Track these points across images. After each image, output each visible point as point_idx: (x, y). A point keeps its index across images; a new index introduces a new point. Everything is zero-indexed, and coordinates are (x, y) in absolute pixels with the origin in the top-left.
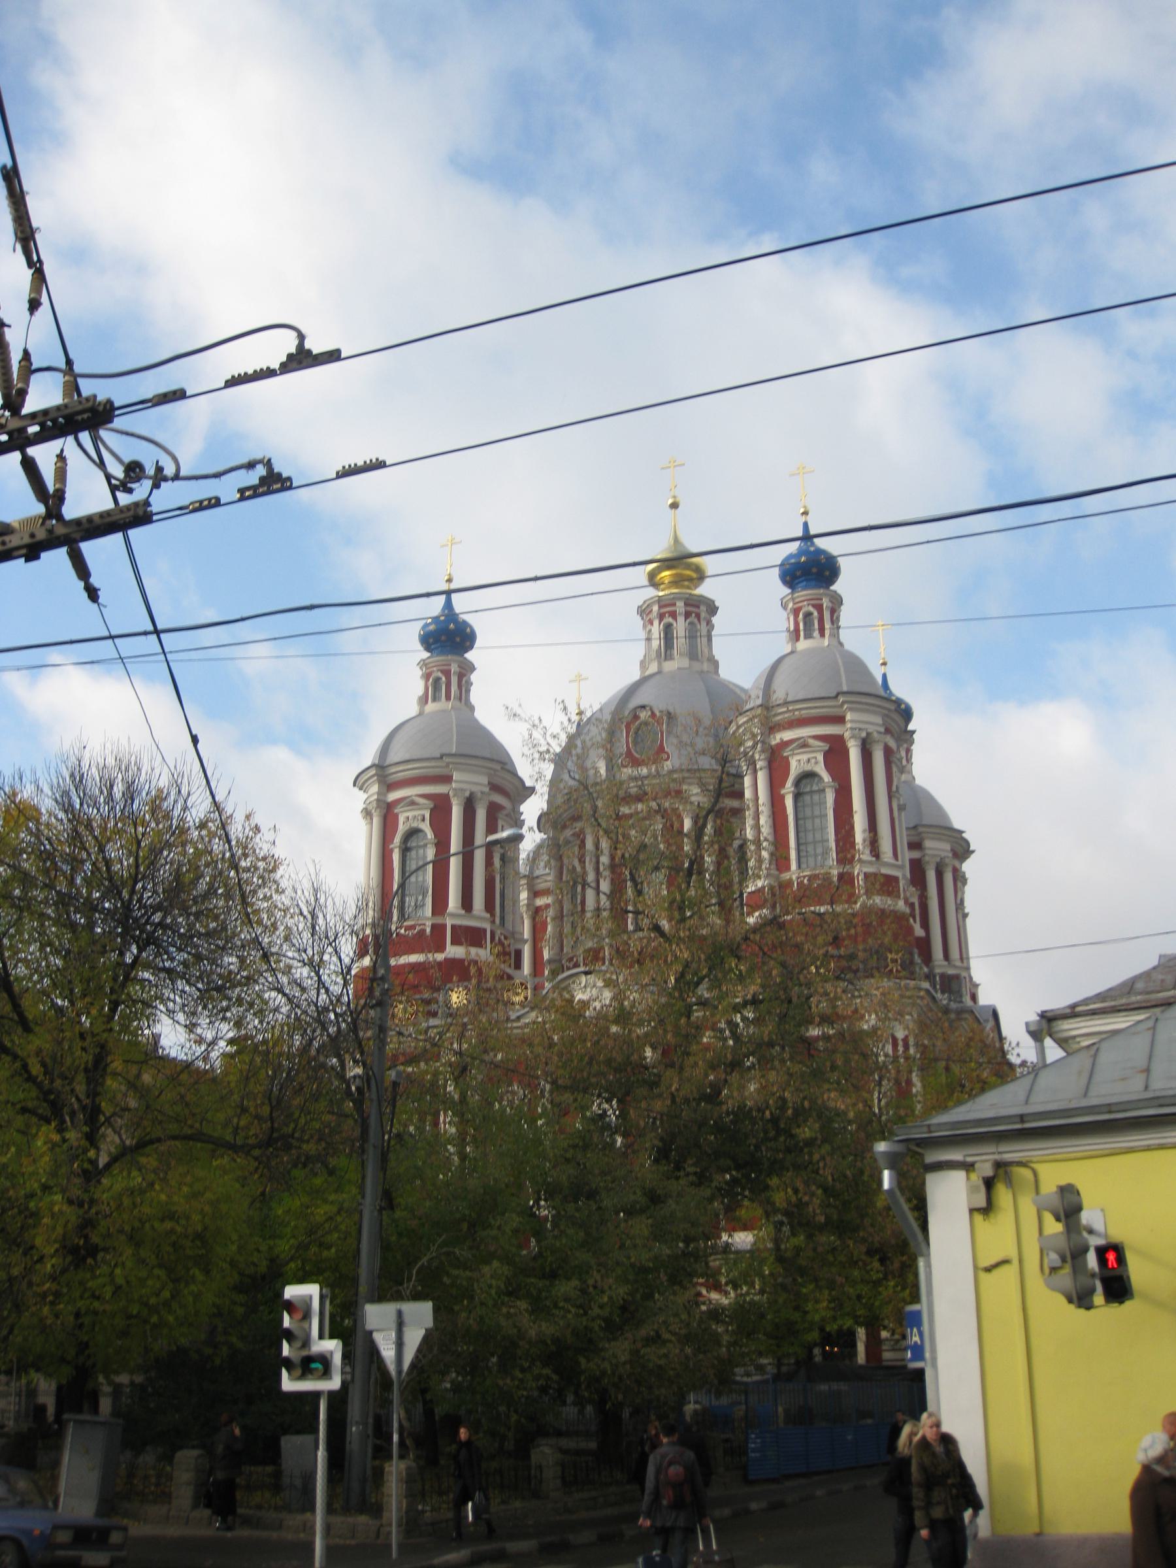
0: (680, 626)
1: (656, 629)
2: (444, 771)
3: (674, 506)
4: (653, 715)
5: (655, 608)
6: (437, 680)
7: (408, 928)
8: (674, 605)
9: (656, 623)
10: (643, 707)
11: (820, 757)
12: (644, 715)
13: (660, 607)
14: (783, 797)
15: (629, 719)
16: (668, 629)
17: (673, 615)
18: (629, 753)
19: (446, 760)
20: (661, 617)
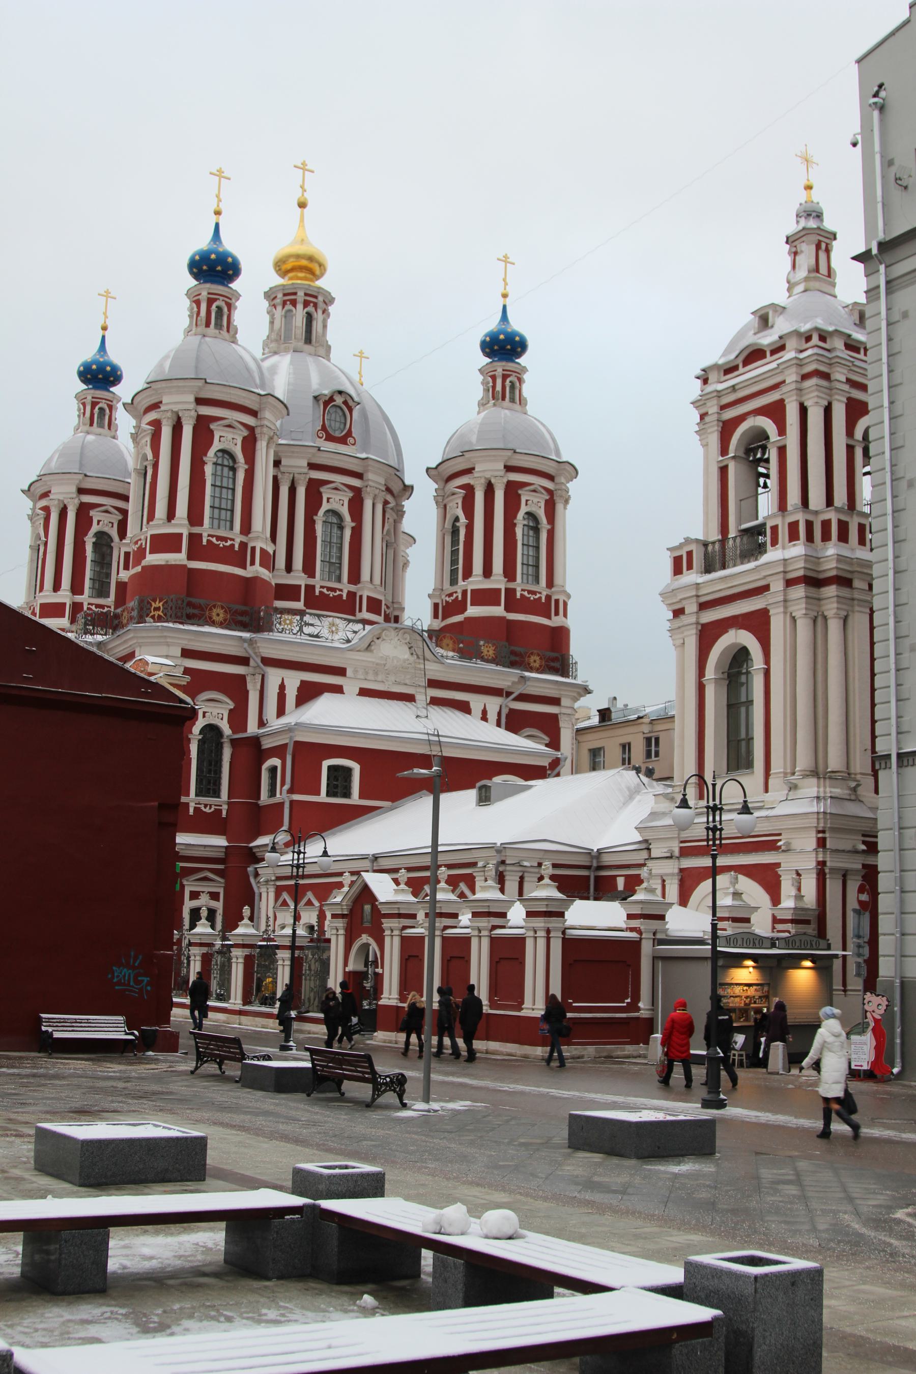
0: (319, 316)
1: (300, 313)
2: (255, 407)
3: (302, 205)
4: (345, 403)
5: (301, 294)
6: (219, 309)
7: (219, 538)
8: (316, 297)
9: (300, 306)
10: (340, 392)
11: (542, 504)
12: (339, 400)
13: (306, 294)
14: (515, 525)
15: (327, 398)
16: (309, 318)
17: (315, 306)
18: (324, 428)
19: (271, 399)
20: (306, 304)
